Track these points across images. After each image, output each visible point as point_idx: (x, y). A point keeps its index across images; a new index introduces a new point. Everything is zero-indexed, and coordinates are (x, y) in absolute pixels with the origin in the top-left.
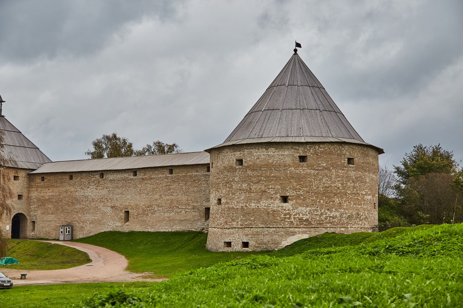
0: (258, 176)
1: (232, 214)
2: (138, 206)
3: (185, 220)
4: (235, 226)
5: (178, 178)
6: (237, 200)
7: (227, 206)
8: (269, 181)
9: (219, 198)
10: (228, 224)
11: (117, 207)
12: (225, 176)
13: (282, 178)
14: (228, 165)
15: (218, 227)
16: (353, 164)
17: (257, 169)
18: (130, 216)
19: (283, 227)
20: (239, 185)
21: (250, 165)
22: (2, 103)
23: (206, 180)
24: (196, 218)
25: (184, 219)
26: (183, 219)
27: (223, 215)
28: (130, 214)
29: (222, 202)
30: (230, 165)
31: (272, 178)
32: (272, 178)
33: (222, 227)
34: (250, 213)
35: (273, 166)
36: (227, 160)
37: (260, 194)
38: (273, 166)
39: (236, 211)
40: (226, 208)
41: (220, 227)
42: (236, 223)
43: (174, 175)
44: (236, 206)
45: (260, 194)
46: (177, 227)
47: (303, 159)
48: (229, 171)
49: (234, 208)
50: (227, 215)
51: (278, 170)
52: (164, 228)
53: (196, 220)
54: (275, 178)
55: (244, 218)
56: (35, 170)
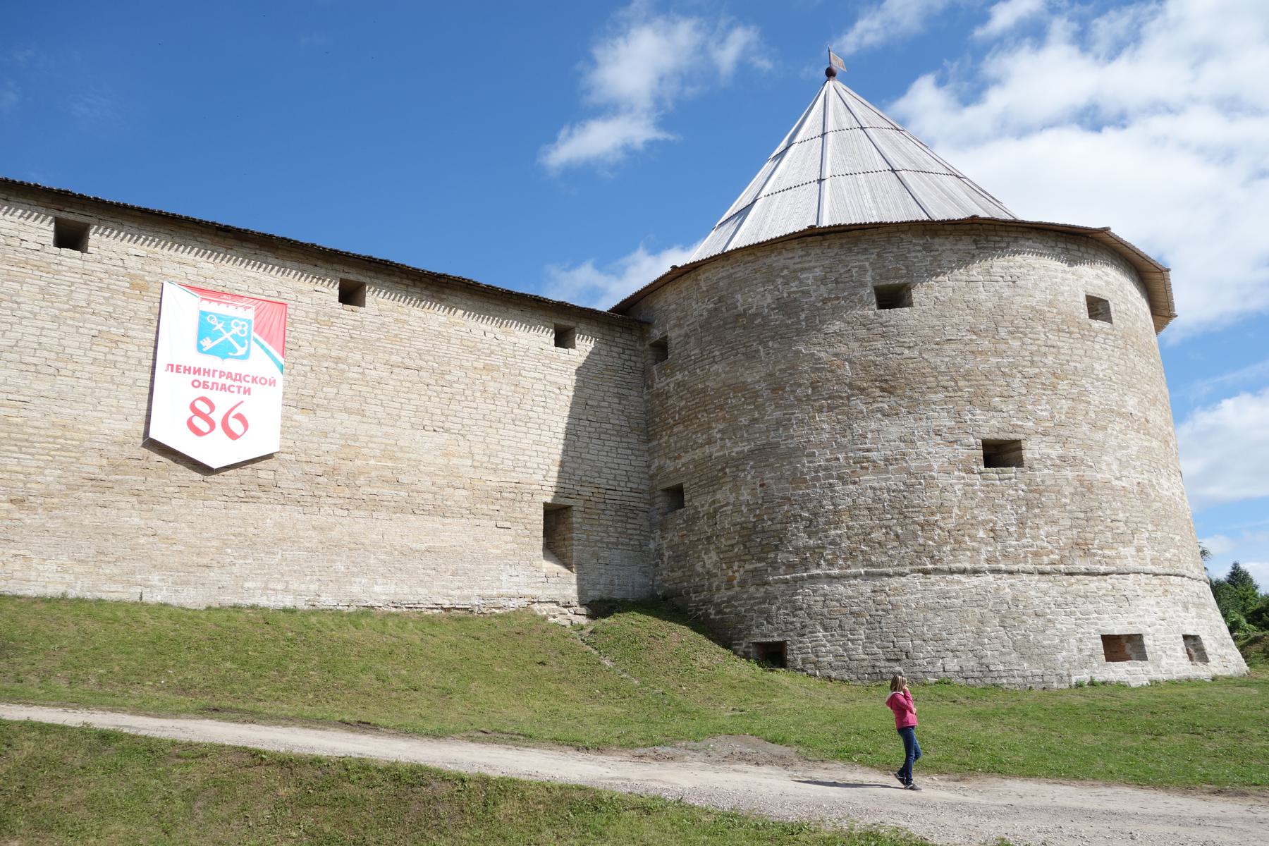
1: (1108, 512)
2: (75, 435)
4: (1131, 564)
5: (396, 336)
6: (1118, 454)
7: (1068, 473)
10: (1095, 555)
12: (1043, 349)
14: (1050, 304)
15: (1015, 568)
20: (1115, 397)
23: (553, 379)
24: (497, 547)
25: (423, 547)
27: (1054, 512)
29: (1027, 455)
30: (1063, 308)
33: (1048, 568)
36: (1042, 285)
40: (1069, 484)
41: (1030, 567)
42: (1130, 551)
44: (1117, 479)
46: (377, 589)
48: (1063, 331)
49: (1112, 488)
50: (1082, 515)
52: (280, 586)
53: (497, 557)
55: (1159, 533)
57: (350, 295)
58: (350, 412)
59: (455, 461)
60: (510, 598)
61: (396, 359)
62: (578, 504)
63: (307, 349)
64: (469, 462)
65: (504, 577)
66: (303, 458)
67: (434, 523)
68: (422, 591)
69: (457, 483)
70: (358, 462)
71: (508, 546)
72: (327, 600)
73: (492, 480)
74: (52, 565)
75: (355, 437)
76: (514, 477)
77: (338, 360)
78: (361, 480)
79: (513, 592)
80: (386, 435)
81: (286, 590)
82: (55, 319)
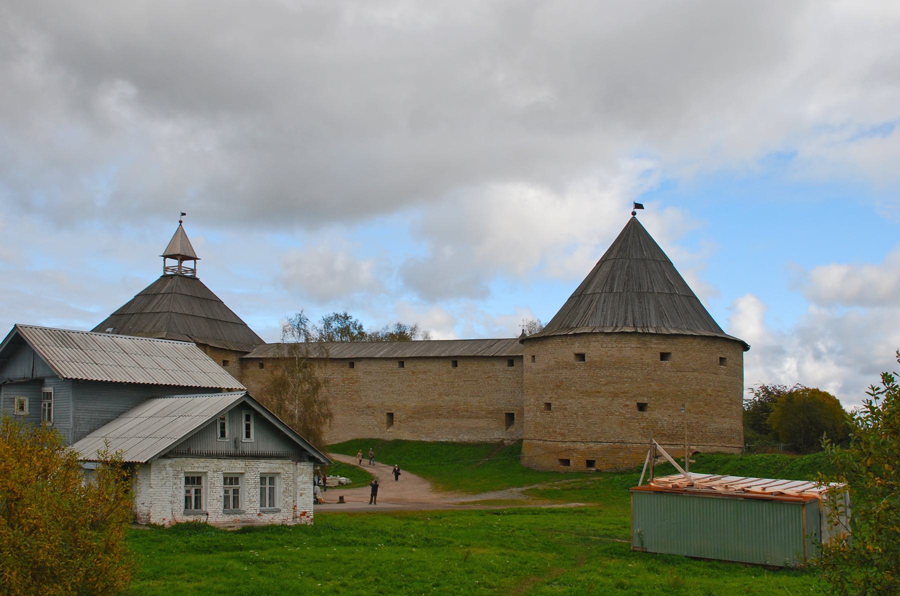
0: (607, 376)
3: (476, 427)
8: (622, 383)
9: (547, 402)
11: (375, 407)
13: (639, 380)
16: (726, 366)
17: (605, 367)
18: (394, 419)
19: (642, 442)
21: (596, 362)
22: (197, 261)
25: (475, 426)
26: (473, 426)
28: (394, 416)
31: (626, 380)
32: (626, 380)
34: (597, 424)
35: (627, 364)
37: (610, 399)
38: (627, 364)
39: (576, 420)
43: (459, 368)
45: (610, 399)
47: (664, 356)
51: (635, 370)
54: (630, 380)
56: (249, 353)
57: (455, 364)
58: (456, 395)
59: (482, 404)
60: (497, 439)
61: (466, 379)
62: (516, 413)
63: (446, 380)
64: (485, 404)
65: (495, 433)
66: (447, 407)
67: (477, 420)
68: (475, 437)
69: (482, 409)
70: (459, 407)
71: (496, 425)
72: (454, 440)
73: (491, 408)
74: (406, 434)
75: (458, 401)
76: (497, 407)
77: (452, 382)
78: (460, 411)
79: (498, 437)
80: (465, 400)
81: (446, 438)
82: (401, 384)
